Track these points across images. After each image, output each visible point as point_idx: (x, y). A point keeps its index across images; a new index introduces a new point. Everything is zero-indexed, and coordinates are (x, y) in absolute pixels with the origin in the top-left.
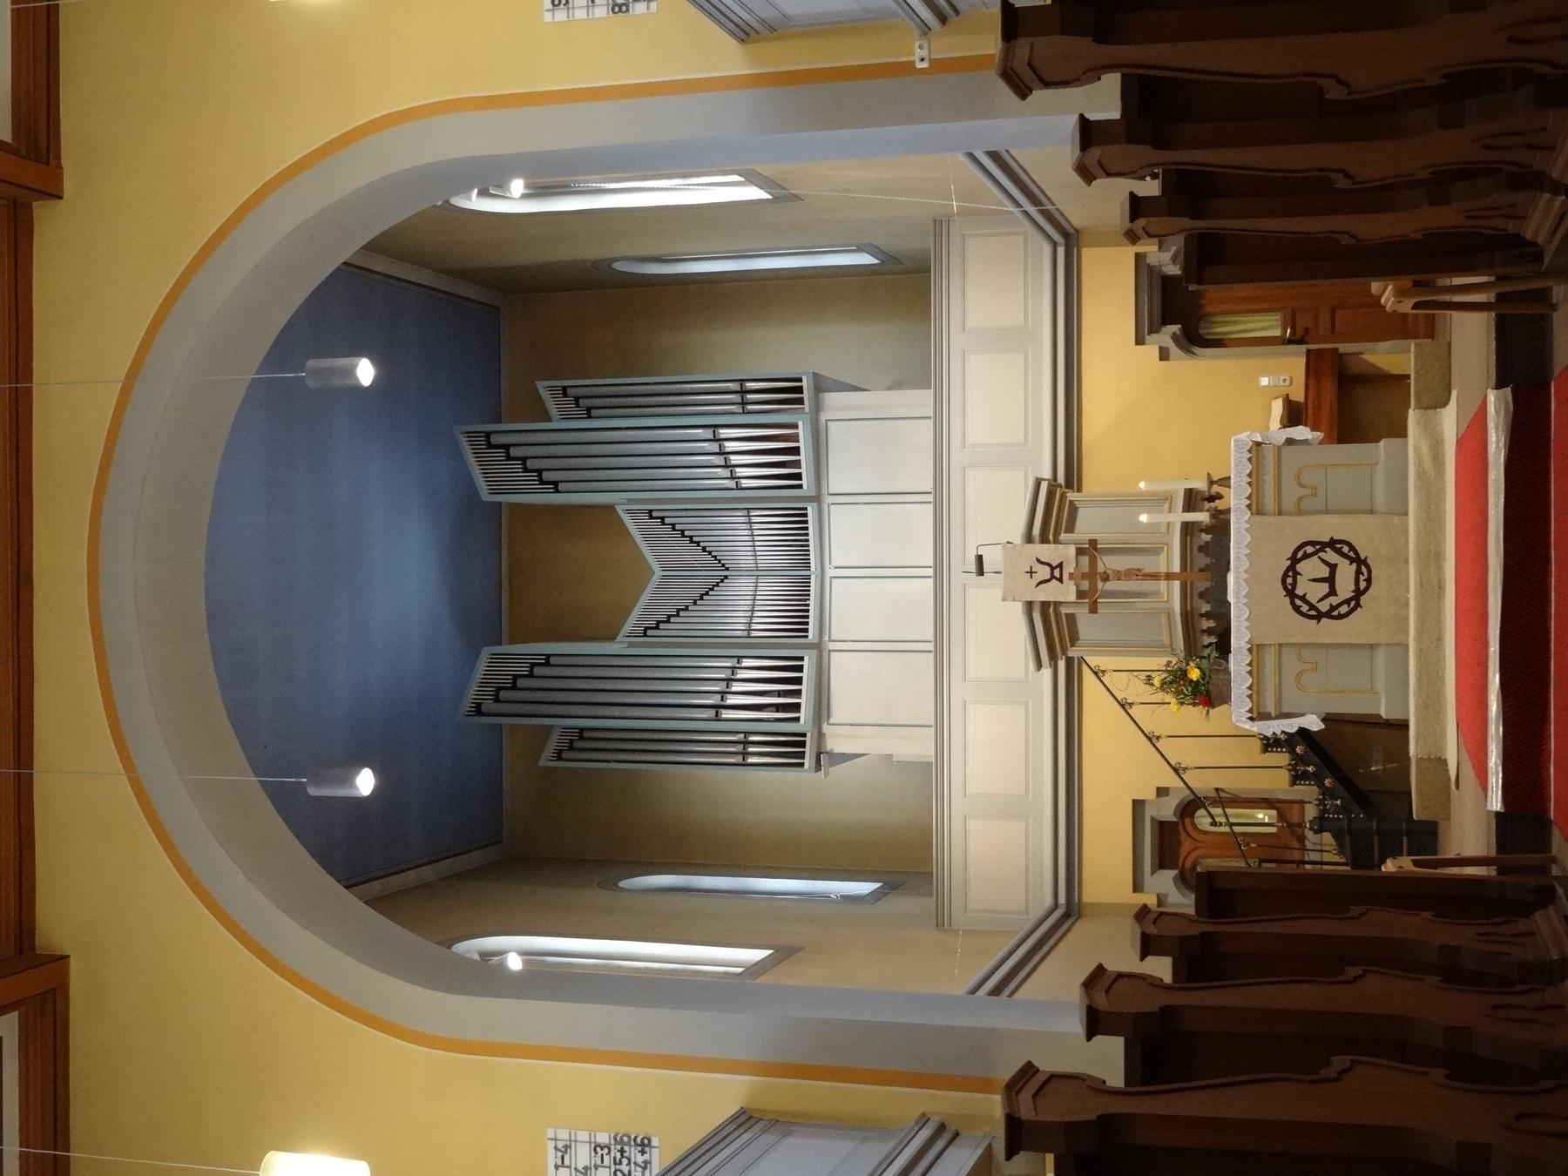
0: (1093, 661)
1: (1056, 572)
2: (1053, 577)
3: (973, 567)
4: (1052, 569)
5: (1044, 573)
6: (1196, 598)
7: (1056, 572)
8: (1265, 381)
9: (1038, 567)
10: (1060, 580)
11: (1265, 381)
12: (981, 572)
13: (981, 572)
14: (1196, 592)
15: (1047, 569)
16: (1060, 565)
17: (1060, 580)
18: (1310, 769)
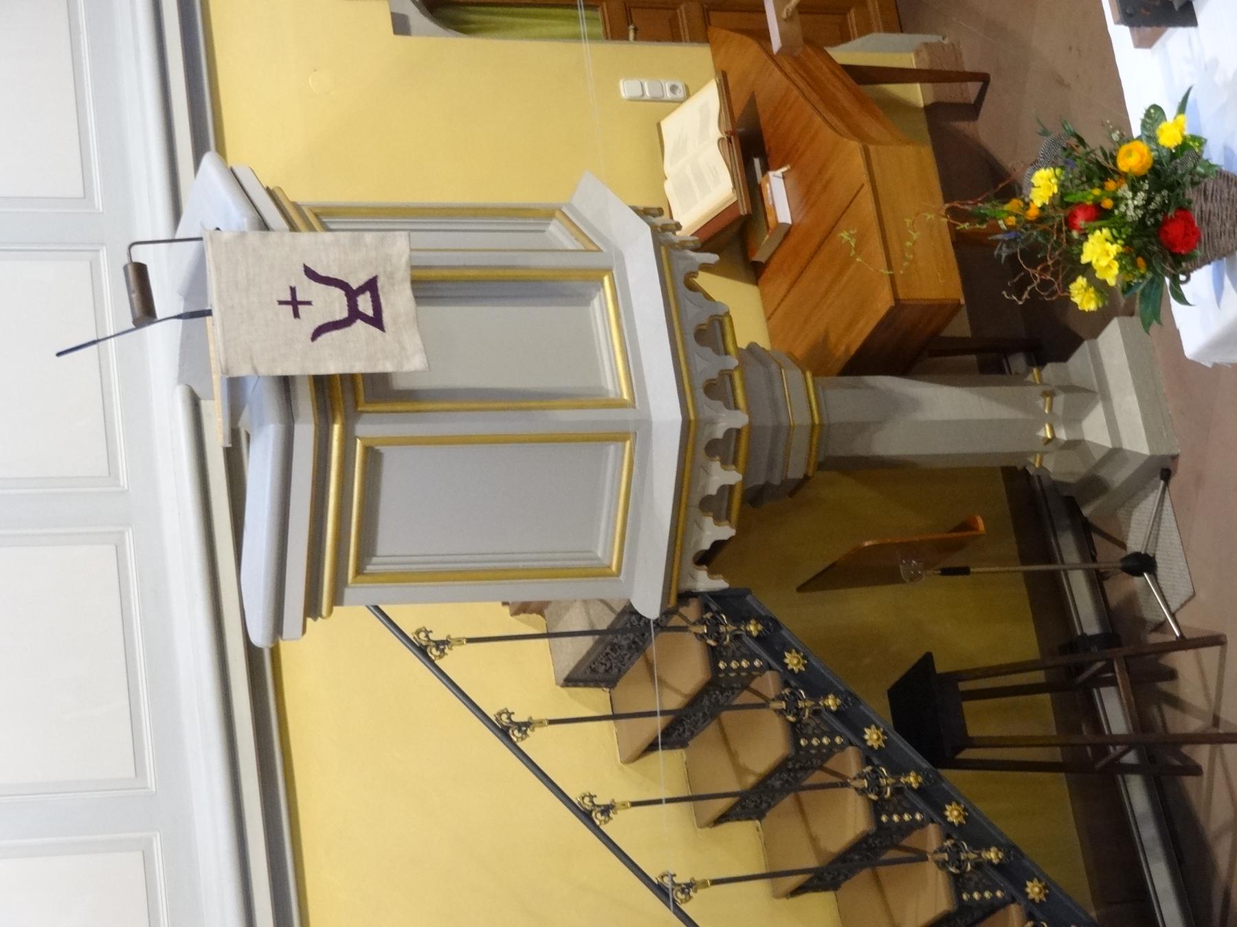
0: (409, 617)
1: (362, 304)
2: (355, 314)
3: (117, 303)
4: (352, 295)
5: (333, 304)
6: (700, 392)
7: (362, 304)
8: (627, 88)
9: (308, 290)
10: (376, 321)
11: (627, 88)
12: (146, 312)
13: (146, 312)
14: (700, 383)
15: (339, 293)
16: (371, 286)
17: (376, 321)
18: (992, 855)
